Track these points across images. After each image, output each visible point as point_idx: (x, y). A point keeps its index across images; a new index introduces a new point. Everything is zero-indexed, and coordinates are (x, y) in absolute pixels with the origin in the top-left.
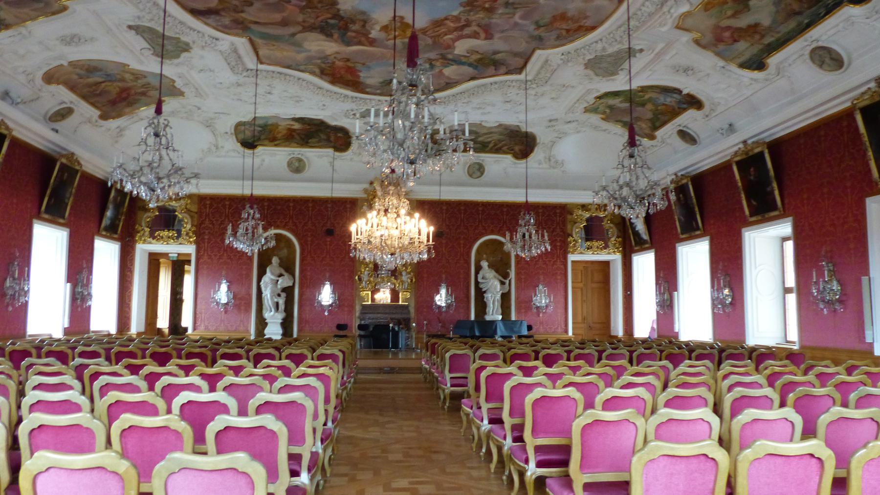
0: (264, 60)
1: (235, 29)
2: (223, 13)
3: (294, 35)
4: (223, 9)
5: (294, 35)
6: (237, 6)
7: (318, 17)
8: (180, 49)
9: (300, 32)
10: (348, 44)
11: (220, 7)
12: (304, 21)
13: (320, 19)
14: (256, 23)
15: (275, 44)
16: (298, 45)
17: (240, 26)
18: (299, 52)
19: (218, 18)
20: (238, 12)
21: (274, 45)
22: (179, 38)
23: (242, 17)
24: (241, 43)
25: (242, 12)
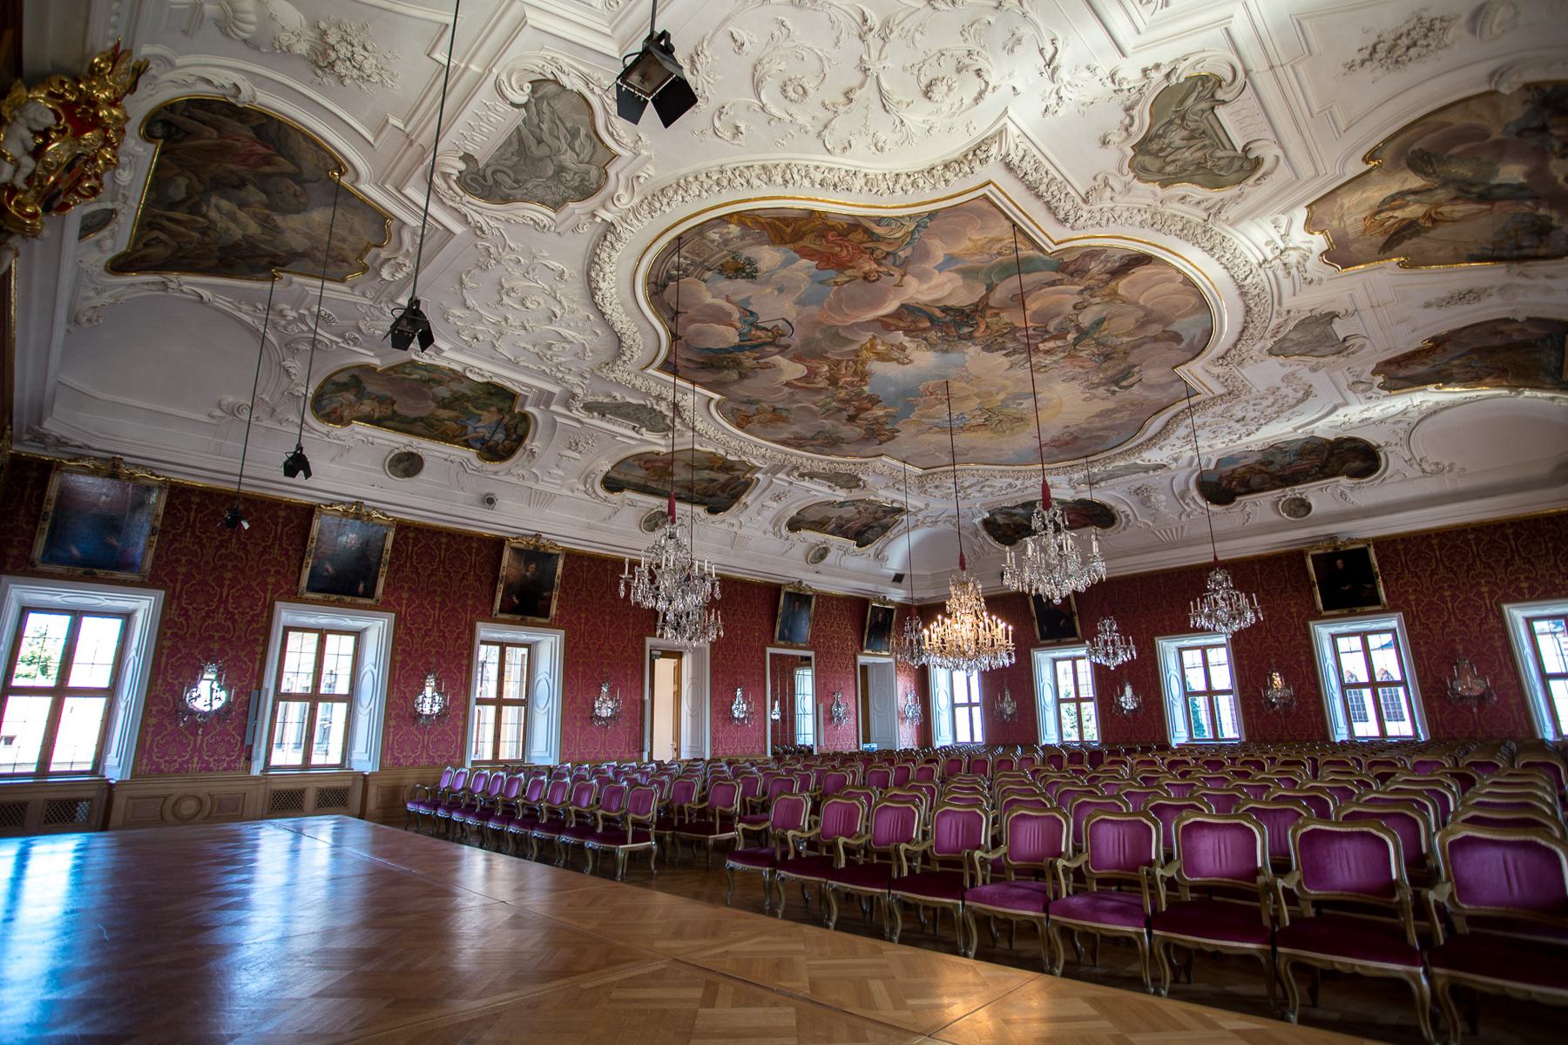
0: (985, 205)
1: (1076, 260)
2: (1105, 277)
3: (990, 288)
4: (1107, 283)
5: (990, 288)
6: (1092, 296)
7: (987, 327)
8: (1154, 147)
9: (986, 298)
10: (903, 306)
11: (1113, 284)
12: (997, 315)
13: (983, 327)
14: (1053, 283)
15: (1000, 258)
16: (968, 274)
17: (1072, 268)
18: (951, 259)
19: (1109, 265)
20: (1086, 289)
21: (999, 254)
22: (1164, 185)
23: (1076, 284)
24: (1052, 236)
25: (1081, 292)
